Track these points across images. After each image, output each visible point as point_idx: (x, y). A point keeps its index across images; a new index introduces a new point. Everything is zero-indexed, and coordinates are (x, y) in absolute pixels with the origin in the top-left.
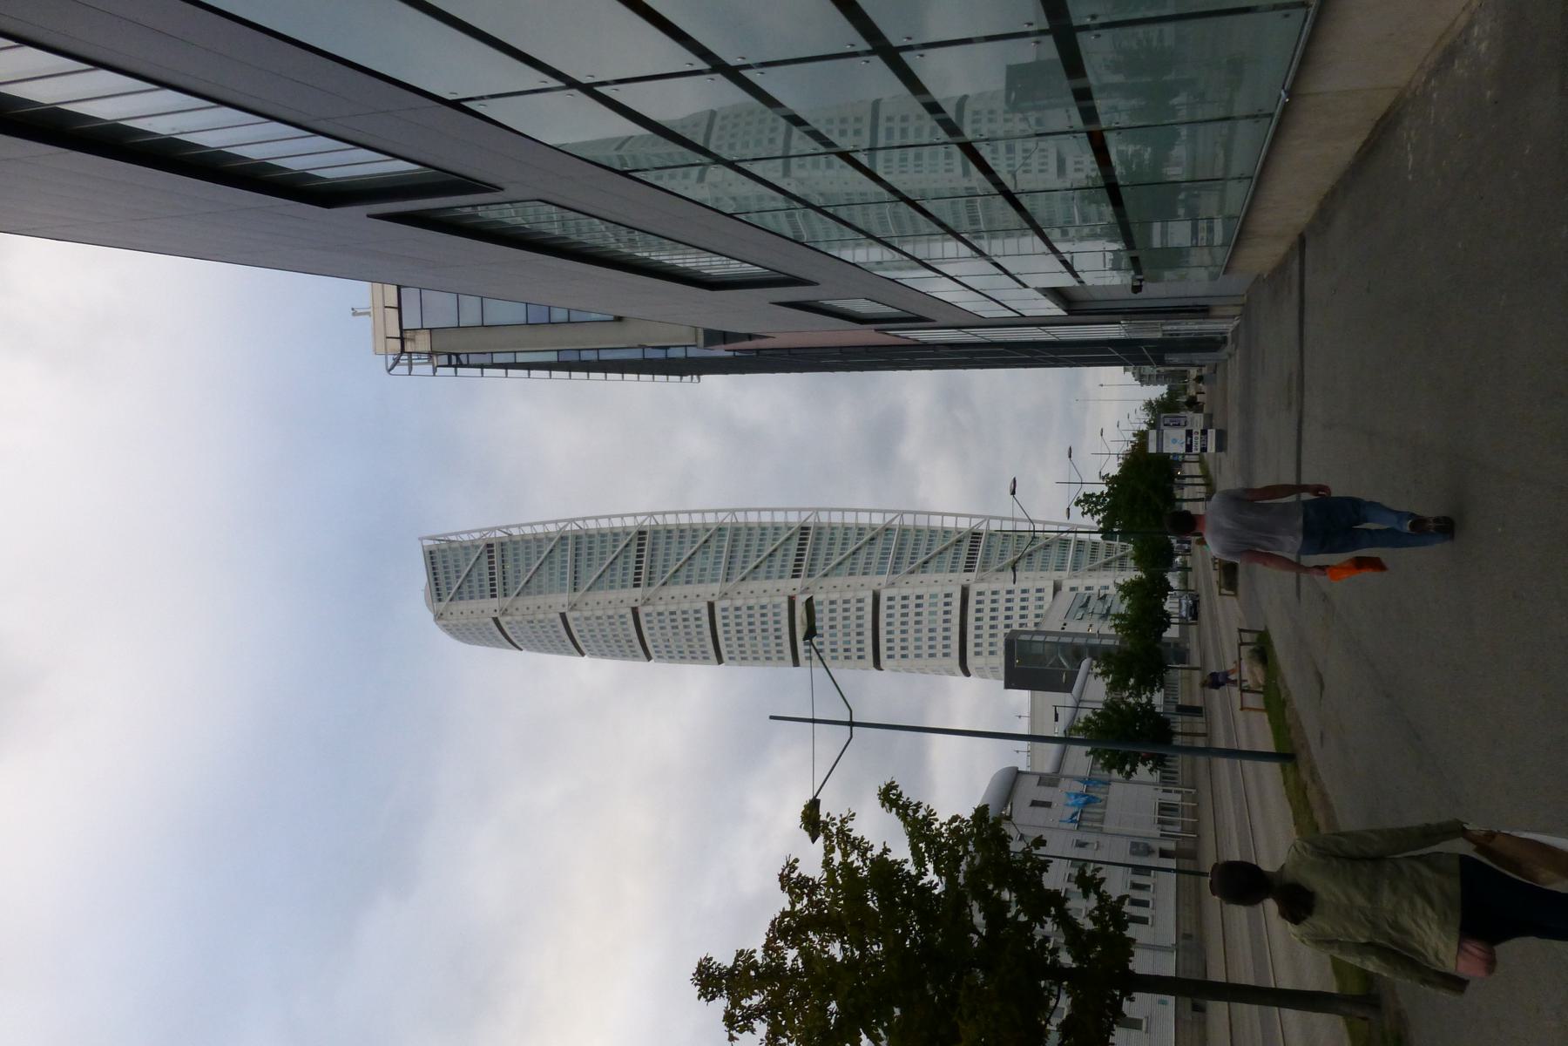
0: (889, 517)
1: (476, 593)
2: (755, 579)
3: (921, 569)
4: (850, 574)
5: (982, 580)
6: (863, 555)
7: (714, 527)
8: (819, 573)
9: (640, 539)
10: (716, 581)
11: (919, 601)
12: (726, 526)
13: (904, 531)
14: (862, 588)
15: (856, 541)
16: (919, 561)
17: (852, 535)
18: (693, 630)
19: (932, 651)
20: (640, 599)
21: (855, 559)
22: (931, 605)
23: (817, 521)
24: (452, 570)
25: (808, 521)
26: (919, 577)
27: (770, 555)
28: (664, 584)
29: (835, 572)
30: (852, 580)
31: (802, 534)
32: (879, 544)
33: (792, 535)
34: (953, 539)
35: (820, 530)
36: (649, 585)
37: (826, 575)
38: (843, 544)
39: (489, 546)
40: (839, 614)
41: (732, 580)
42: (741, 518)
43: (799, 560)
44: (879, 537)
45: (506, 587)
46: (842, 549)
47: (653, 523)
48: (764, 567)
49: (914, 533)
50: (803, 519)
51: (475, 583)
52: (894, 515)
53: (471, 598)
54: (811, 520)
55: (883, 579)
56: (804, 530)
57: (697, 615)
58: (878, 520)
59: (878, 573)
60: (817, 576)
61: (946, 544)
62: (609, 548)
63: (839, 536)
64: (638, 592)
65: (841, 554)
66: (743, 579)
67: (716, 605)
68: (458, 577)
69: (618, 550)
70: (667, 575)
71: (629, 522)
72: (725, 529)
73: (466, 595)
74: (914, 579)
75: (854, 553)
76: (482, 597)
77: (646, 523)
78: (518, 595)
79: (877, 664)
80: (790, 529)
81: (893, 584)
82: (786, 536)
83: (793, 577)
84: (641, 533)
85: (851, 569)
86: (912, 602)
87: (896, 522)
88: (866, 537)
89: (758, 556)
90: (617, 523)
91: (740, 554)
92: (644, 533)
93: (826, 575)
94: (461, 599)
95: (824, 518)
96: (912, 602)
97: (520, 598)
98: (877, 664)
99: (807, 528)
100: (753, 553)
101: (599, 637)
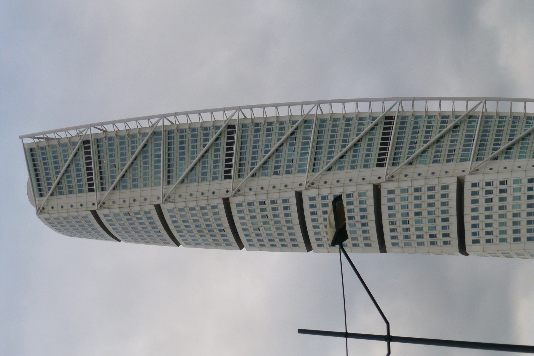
0: (472, 104)
1: (75, 188)
2: (340, 168)
3: (504, 155)
4: (435, 162)
7: (300, 119)
8: (403, 161)
9: (229, 133)
10: (304, 171)
11: (503, 187)
12: (311, 118)
13: (487, 118)
14: (447, 175)
16: (503, 147)
17: (436, 123)
18: (282, 219)
19: (516, 235)
20: (230, 190)
21: (439, 146)
22: (515, 190)
23: (400, 110)
24: (51, 166)
25: (392, 110)
26: (502, 163)
27: (355, 145)
28: (254, 175)
29: (419, 160)
30: (436, 167)
32: (463, 131)
33: (376, 124)
36: (239, 176)
37: (410, 163)
38: (427, 132)
39: (86, 142)
40: (424, 202)
41: (318, 170)
42: (326, 109)
44: (462, 125)
45: (103, 181)
46: (426, 137)
47: (242, 117)
48: (349, 157)
50: (386, 110)
51: (74, 179)
52: (475, 103)
53: (71, 192)
54: (395, 109)
55: (467, 165)
56: (388, 119)
57: (286, 205)
58: (461, 108)
59: (461, 160)
60: (401, 165)
62: (200, 143)
63: (423, 124)
64: (229, 184)
65: (425, 142)
66: (329, 169)
67: (303, 194)
68: (57, 173)
69: (209, 144)
70: (256, 167)
71: (219, 116)
72: (311, 121)
73: (65, 189)
74: (498, 165)
75: (438, 141)
76: (81, 191)
77: (235, 117)
78: (114, 189)
79: (462, 249)
80: (374, 119)
81: (477, 170)
82: (371, 126)
83: (378, 165)
84: (231, 127)
85: (435, 156)
86: (496, 188)
87: (479, 109)
88: (450, 125)
89: (344, 146)
90: (207, 118)
91: (326, 145)
92: (233, 126)
93: (410, 163)
94: (61, 193)
95: (407, 107)
96: (496, 188)
97: (117, 191)
98: (462, 249)
99: (392, 118)
100: (339, 143)
101: (193, 227)
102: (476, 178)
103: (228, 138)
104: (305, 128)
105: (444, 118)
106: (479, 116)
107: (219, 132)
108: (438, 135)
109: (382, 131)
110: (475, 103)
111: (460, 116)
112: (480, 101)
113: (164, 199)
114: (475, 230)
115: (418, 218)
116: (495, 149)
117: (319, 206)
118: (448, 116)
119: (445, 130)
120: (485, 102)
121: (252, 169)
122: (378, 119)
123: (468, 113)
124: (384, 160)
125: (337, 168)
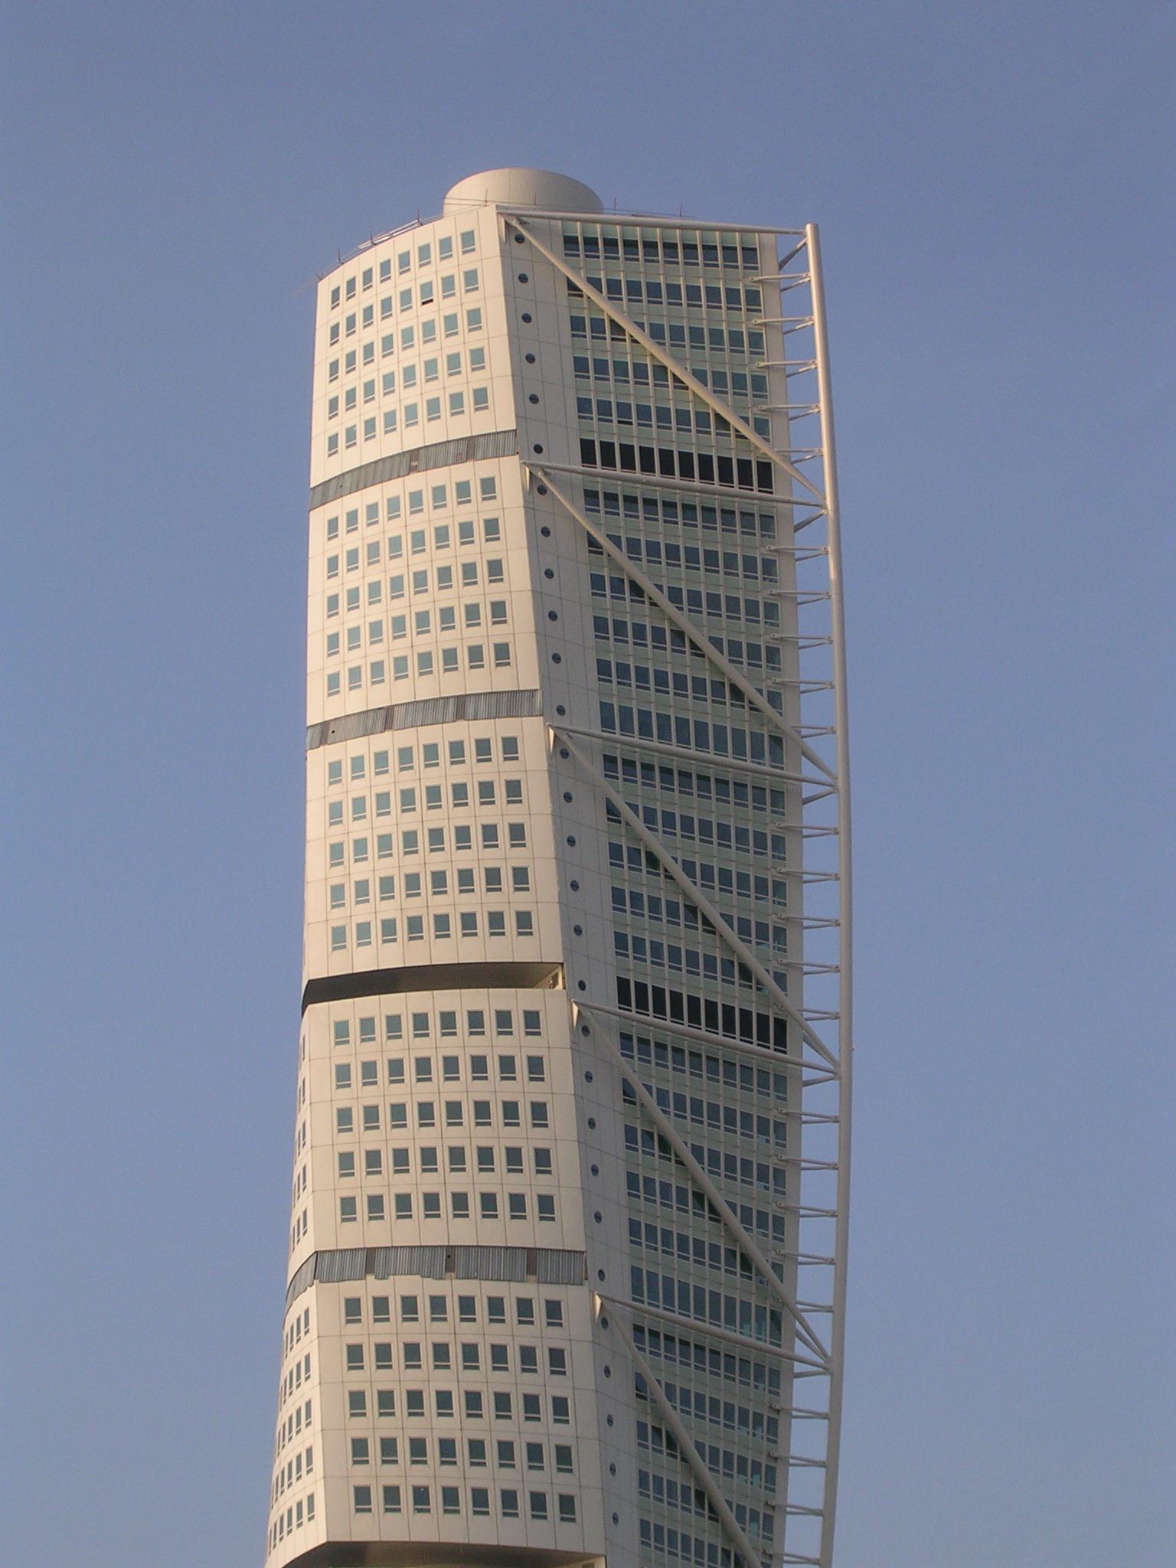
0: (821, 1325)
6: (695, 1226)
8: (633, 1070)
15: (739, 1201)
17: (755, 1195)
35: (778, 1083)
36: (591, 496)
37: (628, 1094)
54: (809, 1054)
59: (636, 1273)
60: (605, 783)
61: (731, 1516)
72: (777, 758)
80: (780, 979)
83: (623, 984)
87: (800, 1349)
88: (751, 1241)
89: (688, 867)
92: (766, 481)
95: (819, 1099)
99: (781, 1042)
100: (699, 852)
104: (757, 738)
105: (777, 1225)
112: (829, 1352)
116: (670, 1389)
118: (782, 1240)
119: (735, 1221)
121: (616, 540)
122: (782, 993)
124: (642, 1005)
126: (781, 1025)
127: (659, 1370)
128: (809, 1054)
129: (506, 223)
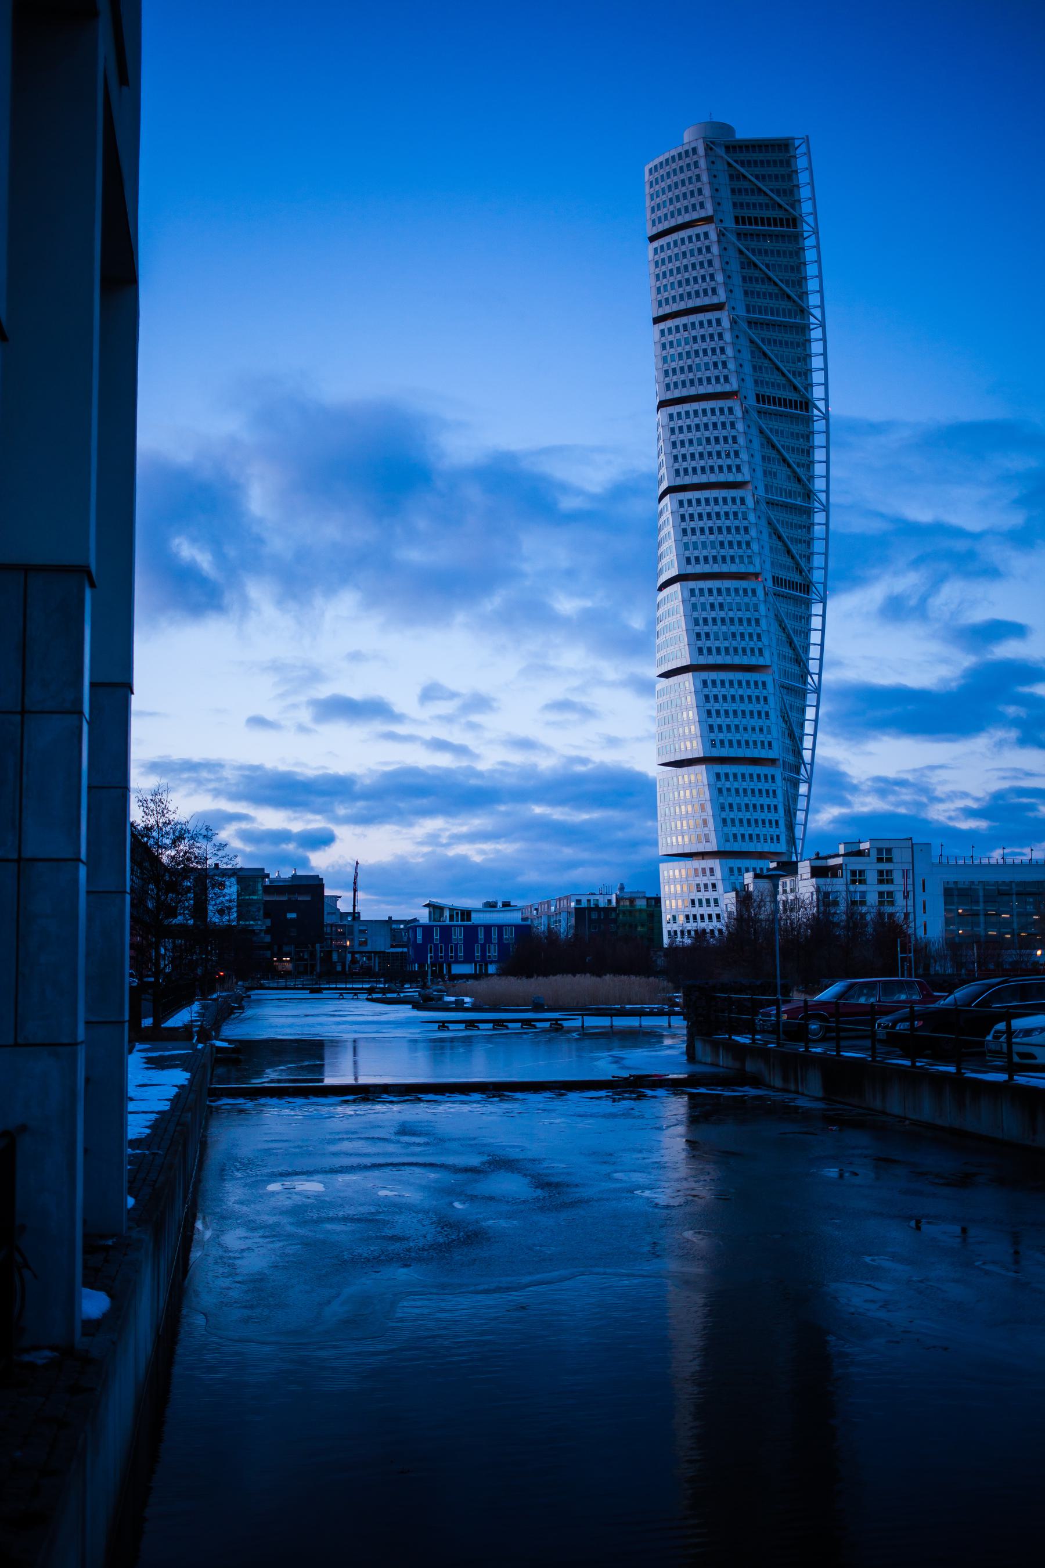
4: (763, 458)
5: (766, 594)
7: (804, 306)
9: (788, 220)
10: (748, 311)
27: (770, 279)
31: (801, 402)
34: (803, 563)
41: (750, 327)
42: (816, 334)
43: (776, 401)
44: (800, 486)
47: (806, 235)
49: (807, 539)
50: (817, 403)
52: (824, 500)
54: (816, 412)
58: (819, 484)
71: (806, 208)
77: (806, 227)
83: (757, 395)
84: (794, 222)
87: (817, 504)
90: (804, 193)
93: (761, 432)
98: (662, 404)
102: (760, 593)
103: (781, 220)
105: (810, 465)
106: (810, 504)
107: (788, 208)
108: (791, 461)
109: (793, 399)
110: (824, 500)
111: (809, 482)
113: (709, 143)
114: (694, 503)
115: (704, 441)
117: (711, 330)
119: (795, 466)
120: (824, 511)
123: (813, 493)
125: (743, 260)
126: (807, 404)
127: (774, 515)
128: (816, 412)
129: (707, 145)
